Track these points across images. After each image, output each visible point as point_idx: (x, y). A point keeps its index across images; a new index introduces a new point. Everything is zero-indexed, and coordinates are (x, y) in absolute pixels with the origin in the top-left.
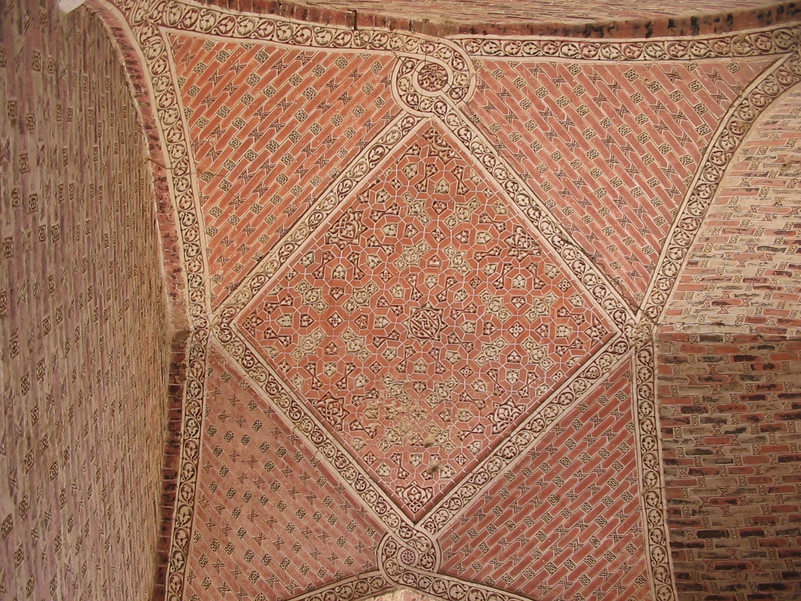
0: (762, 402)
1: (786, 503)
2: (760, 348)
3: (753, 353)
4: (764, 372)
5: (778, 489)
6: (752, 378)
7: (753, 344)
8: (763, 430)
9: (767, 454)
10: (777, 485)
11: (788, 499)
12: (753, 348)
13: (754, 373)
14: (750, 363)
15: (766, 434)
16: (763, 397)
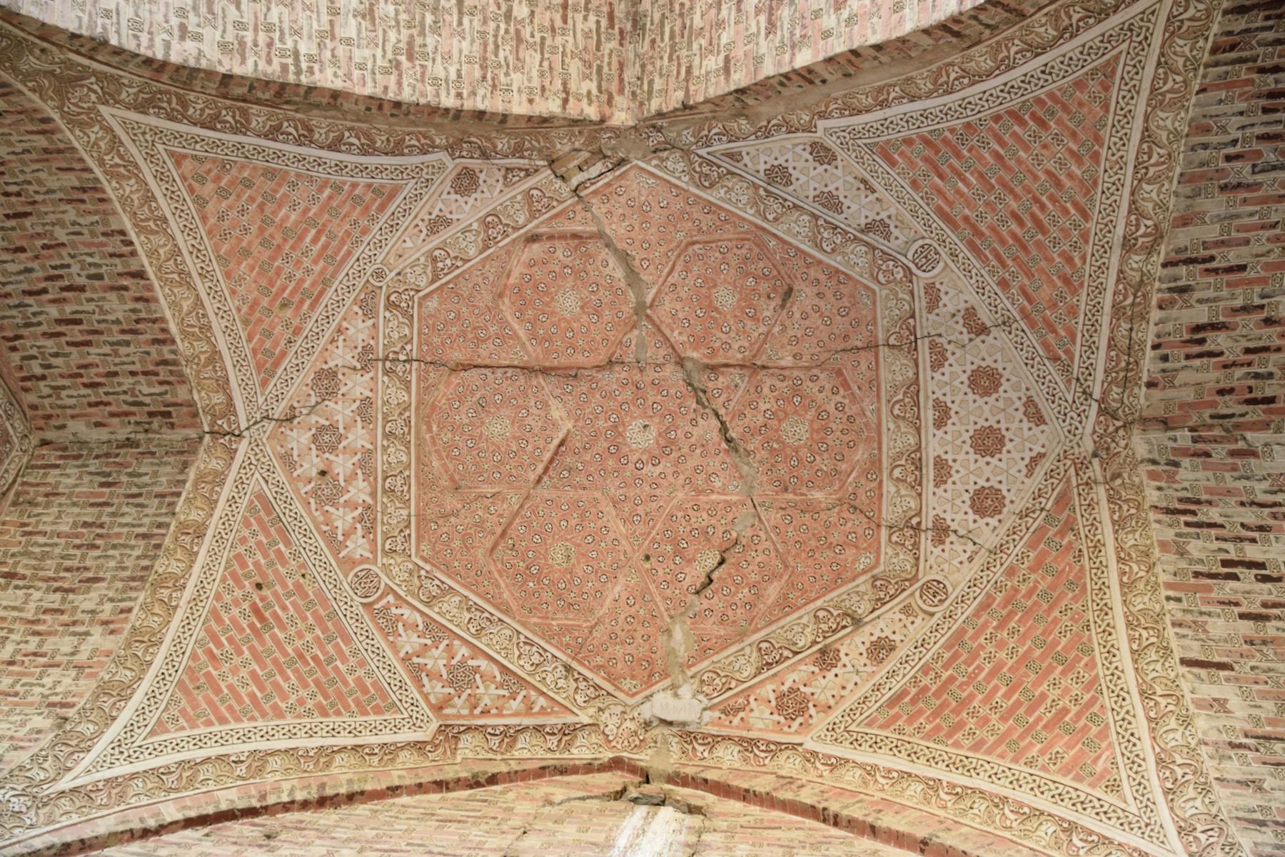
0: (1252, 345)
1: (1258, 208)
2: (1232, 416)
3: (1244, 408)
4: (1235, 384)
5: (1263, 227)
6: (1257, 376)
7: (1241, 420)
8: (1262, 307)
9: (1263, 274)
10: (1261, 232)
11: (1252, 215)
12: (1242, 415)
13: (1252, 382)
14: (1252, 395)
15: (1257, 301)
16: (1248, 351)
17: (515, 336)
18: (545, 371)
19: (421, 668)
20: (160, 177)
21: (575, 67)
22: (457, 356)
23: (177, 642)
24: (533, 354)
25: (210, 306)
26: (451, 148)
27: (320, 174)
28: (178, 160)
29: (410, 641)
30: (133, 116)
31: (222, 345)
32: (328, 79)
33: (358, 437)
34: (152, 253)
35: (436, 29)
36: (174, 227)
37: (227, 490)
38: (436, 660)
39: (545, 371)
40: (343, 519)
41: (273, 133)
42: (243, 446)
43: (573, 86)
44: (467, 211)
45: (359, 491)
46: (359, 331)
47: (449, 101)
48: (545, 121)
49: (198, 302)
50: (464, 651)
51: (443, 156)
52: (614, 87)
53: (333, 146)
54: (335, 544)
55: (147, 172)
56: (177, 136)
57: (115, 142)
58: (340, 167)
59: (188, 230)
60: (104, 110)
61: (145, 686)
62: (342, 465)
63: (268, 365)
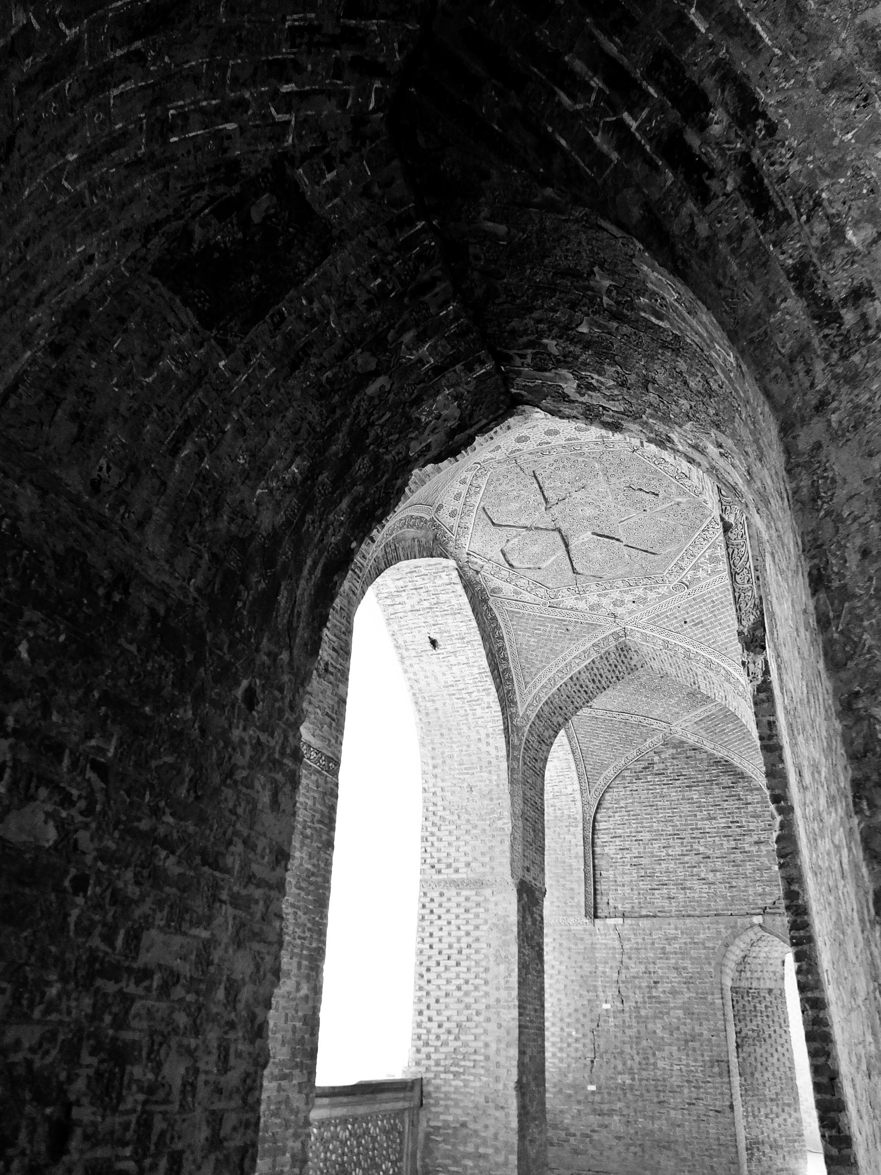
17: (556, 560)
18: (567, 545)
19: (713, 571)
20: (535, 686)
21: (438, 582)
22: (571, 573)
23: (710, 653)
24: (562, 552)
25: (576, 653)
26: (485, 601)
27: (513, 638)
28: (527, 683)
29: (701, 574)
30: (519, 704)
31: (590, 644)
32: (485, 663)
33: (615, 594)
34: (562, 678)
35: (449, 632)
36: (551, 675)
37: (649, 633)
38: (709, 567)
39: (567, 545)
40: (651, 595)
41: (505, 659)
42: (629, 627)
43: (447, 581)
44: (508, 589)
45: (639, 592)
46: (569, 601)
47: (474, 624)
48: (465, 587)
49: (575, 657)
50: (703, 559)
51: (490, 603)
52: (440, 566)
53: (502, 638)
54: (663, 597)
55: (535, 691)
56: (519, 688)
57: (529, 706)
58: (508, 633)
59: (550, 670)
60: (521, 714)
61: (726, 667)
62: (628, 598)
63: (593, 626)
